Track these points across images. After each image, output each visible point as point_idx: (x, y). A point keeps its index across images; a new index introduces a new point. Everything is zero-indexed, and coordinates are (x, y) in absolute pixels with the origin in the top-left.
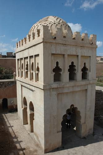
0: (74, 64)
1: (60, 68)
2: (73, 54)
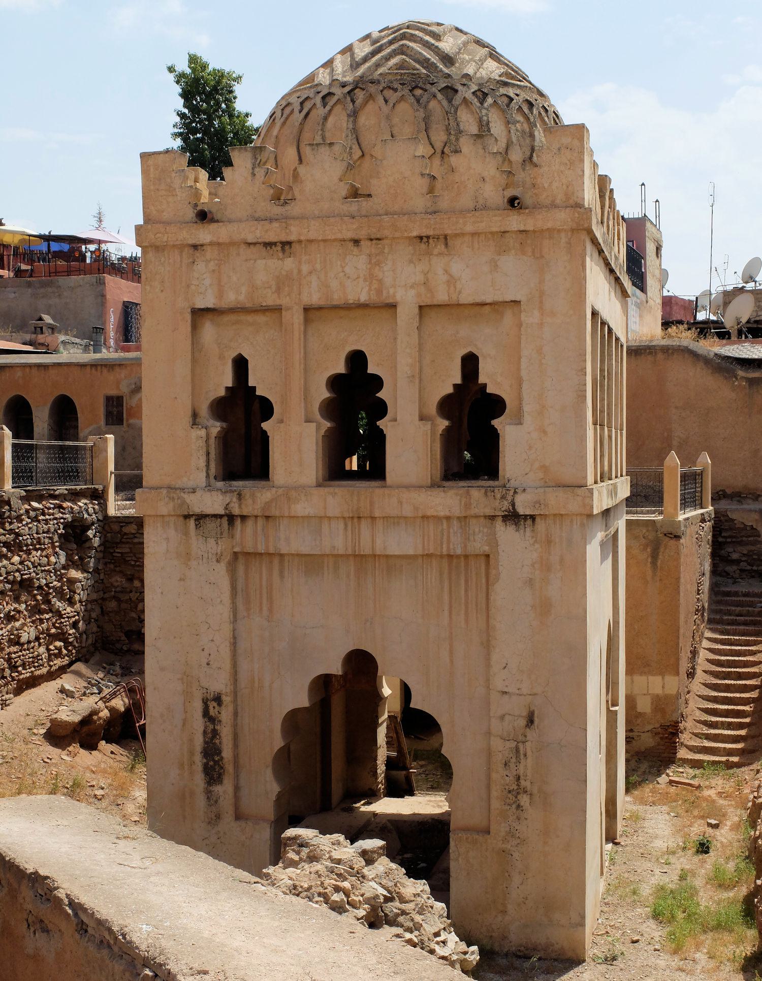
0: (371, 370)
1: (258, 392)
2: (351, 298)
